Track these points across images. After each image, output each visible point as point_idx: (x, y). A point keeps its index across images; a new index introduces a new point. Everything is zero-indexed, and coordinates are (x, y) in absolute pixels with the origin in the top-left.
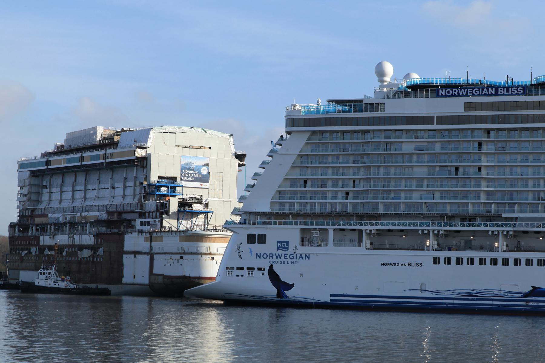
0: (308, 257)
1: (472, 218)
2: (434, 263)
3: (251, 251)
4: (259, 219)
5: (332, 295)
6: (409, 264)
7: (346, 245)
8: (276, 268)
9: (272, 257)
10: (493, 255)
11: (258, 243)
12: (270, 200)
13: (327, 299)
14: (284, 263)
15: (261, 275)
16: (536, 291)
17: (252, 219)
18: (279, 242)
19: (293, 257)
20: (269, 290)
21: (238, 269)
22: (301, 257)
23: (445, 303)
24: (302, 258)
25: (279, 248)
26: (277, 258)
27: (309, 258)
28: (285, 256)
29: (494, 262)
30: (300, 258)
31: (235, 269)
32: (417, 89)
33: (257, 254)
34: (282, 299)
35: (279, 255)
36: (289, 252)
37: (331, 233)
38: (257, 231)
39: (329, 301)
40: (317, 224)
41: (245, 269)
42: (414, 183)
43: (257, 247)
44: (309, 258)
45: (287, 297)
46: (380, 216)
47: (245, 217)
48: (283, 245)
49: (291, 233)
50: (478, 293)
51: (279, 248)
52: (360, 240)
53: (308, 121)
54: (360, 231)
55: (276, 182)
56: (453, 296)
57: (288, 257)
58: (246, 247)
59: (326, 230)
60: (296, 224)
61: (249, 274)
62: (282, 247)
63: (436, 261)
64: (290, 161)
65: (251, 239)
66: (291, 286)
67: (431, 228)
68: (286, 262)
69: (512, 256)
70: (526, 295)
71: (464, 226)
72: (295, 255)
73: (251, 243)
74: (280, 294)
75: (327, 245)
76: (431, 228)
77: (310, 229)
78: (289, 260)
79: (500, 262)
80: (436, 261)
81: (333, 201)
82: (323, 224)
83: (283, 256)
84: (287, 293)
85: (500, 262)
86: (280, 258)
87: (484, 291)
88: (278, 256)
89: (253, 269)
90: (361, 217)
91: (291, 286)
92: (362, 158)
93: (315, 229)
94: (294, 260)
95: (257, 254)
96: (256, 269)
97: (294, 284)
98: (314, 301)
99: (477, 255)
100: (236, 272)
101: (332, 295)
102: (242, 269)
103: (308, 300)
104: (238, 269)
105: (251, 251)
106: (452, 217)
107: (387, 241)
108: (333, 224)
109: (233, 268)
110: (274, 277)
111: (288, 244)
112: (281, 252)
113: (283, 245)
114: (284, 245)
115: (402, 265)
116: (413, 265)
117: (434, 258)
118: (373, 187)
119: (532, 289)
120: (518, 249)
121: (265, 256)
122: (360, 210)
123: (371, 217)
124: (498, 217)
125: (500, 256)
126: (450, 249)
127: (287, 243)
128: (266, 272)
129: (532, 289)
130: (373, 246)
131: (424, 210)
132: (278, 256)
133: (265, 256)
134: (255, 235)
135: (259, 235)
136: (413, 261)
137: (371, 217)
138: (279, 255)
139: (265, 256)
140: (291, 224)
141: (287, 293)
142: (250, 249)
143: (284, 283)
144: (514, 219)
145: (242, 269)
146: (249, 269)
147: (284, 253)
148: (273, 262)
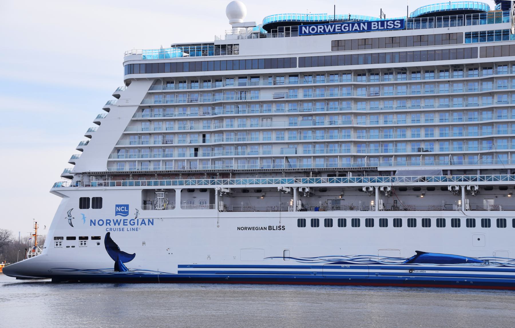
0: (151, 222)
1: (343, 173)
2: (299, 226)
3: (84, 218)
4: (94, 180)
5: (180, 266)
6: (270, 228)
7: (196, 208)
8: (114, 237)
9: (109, 223)
10: (369, 214)
11: (93, 207)
12: (107, 159)
13: (174, 271)
14: (123, 230)
15: (96, 245)
16: (420, 257)
17: (86, 180)
18: (117, 206)
19: (134, 223)
20: (105, 263)
21: (69, 238)
22: (143, 222)
23: (312, 273)
24: (145, 223)
25: (117, 213)
26: (115, 224)
27: (152, 224)
28: (124, 222)
29: (370, 223)
30: (142, 223)
31: (65, 238)
32: (273, 28)
33: (91, 221)
34: (121, 273)
35: (117, 220)
36: (129, 218)
37: (178, 194)
38: (91, 194)
39: (177, 273)
40: (162, 184)
41: (77, 238)
42: (271, 136)
43: (91, 213)
44: (152, 224)
45: (126, 269)
46: (235, 174)
47: (76, 179)
48: (123, 210)
49: (132, 195)
50: (352, 260)
51: (117, 213)
52: (212, 201)
53: (150, 68)
54: (212, 191)
55: (112, 136)
56: (322, 264)
57: (128, 223)
58: (78, 212)
59: (173, 191)
60: (137, 184)
61: (82, 244)
62: (121, 212)
63: (302, 223)
64: (130, 113)
65: (84, 203)
66: (130, 257)
67: (295, 185)
68: (125, 229)
69: (391, 215)
70: (410, 261)
71: (333, 182)
72: (136, 221)
73: (84, 208)
74: (118, 267)
75: (174, 208)
76: (295, 185)
77: (153, 191)
78: (129, 226)
79: (377, 223)
80: (302, 223)
81: (180, 158)
82: (169, 184)
83: (122, 222)
84: (127, 265)
85: (377, 223)
86: (119, 224)
87: (359, 257)
88: (117, 222)
89: (86, 238)
90: (212, 174)
91: (130, 257)
92: (213, 109)
93: (159, 190)
94: (136, 226)
95: (91, 221)
96: (90, 238)
97: (135, 254)
98: (159, 273)
99: (349, 215)
100: (65, 242)
101: (180, 266)
102: (74, 238)
103: (152, 273)
104: (69, 238)
105: (84, 218)
106: (318, 173)
107: (242, 203)
108: (181, 184)
109: (62, 238)
110: (111, 247)
111: (128, 209)
112: (119, 217)
113: (123, 210)
114: (123, 209)
115: (262, 228)
116: (275, 228)
117: (299, 220)
118: (226, 141)
119: (416, 254)
120: (395, 208)
121: (101, 223)
122: (209, 167)
123: (224, 174)
124: (372, 171)
125: (377, 215)
126: (317, 209)
127: (127, 206)
128: (102, 241)
129: (416, 254)
130: (227, 209)
131: (283, 165)
132: (117, 222)
133: (101, 223)
134: (89, 198)
135: (93, 198)
136: (275, 224)
137: (224, 174)
138: (117, 220)
139: (101, 223)
140: (131, 184)
141: (127, 265)
142: (84, 215)
144: (392, 173)
145: (74, 238)
146: (81, 238)
147: (123, 218)
148: (111, 229)
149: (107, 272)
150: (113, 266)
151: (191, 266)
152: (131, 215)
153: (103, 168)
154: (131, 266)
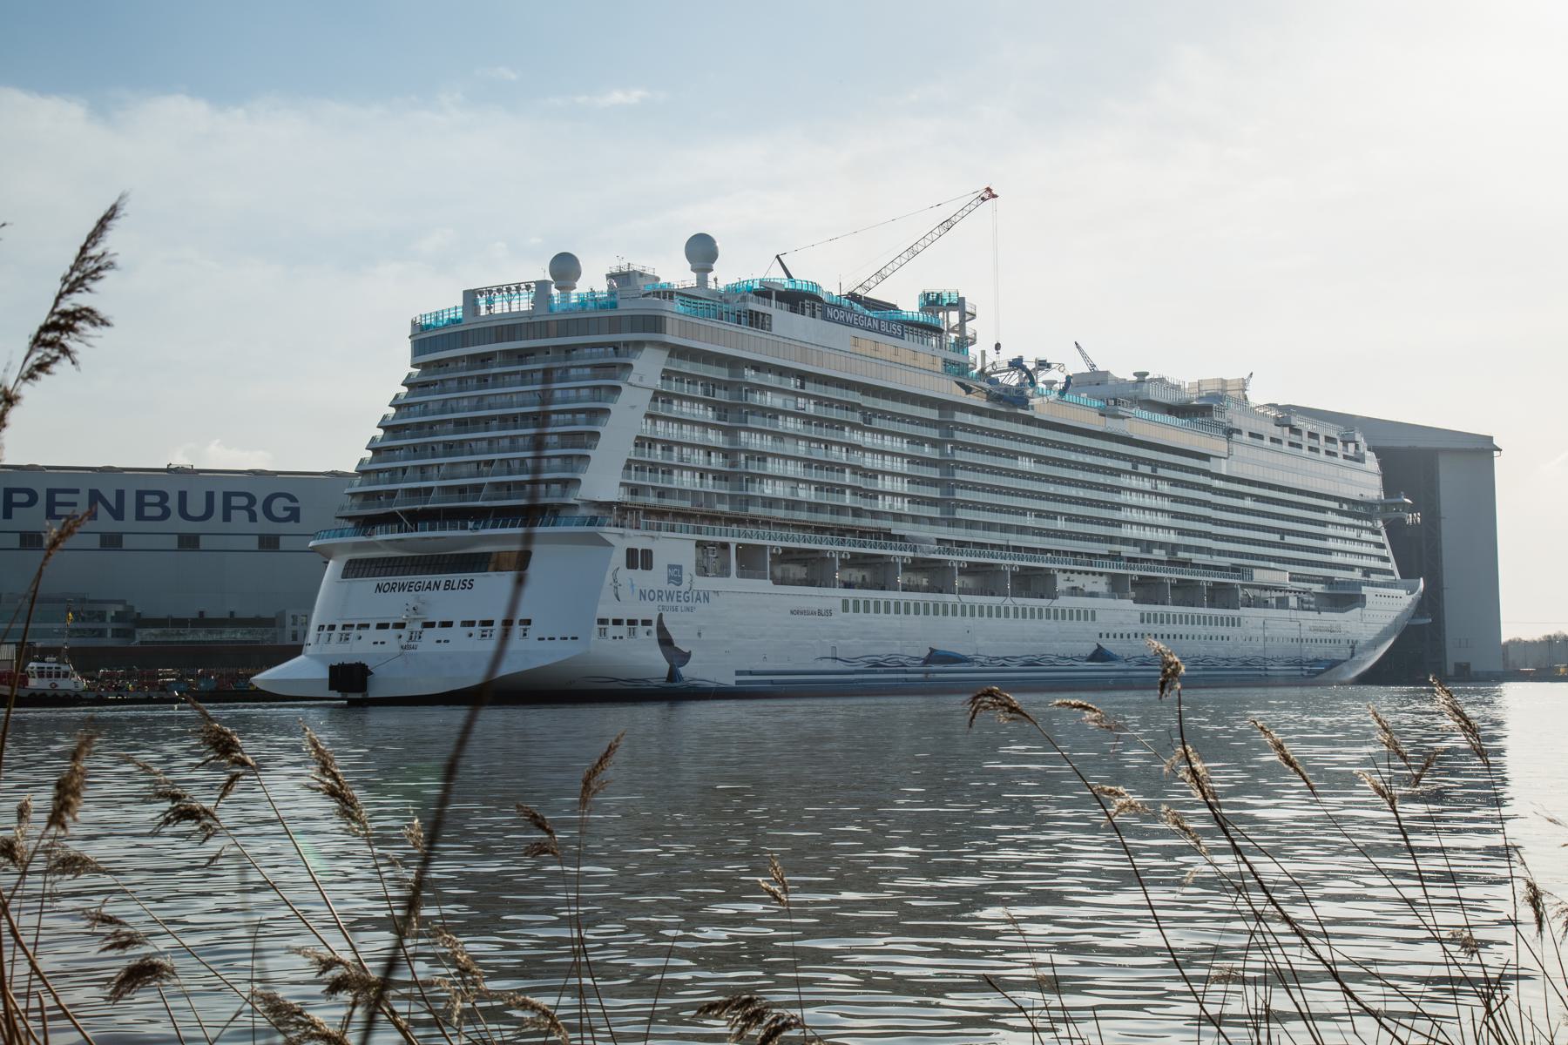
13: (730, 681)
16: (935, 657)
18: (670, 567)
22: (698, 599)
39: (733, 684)
45: (681, 678)
58: (626, 575)
74: (673, 675)
87: (890, 657)
88: (670, 596)
91: (687, 656)
94: (690, 604)
100: (612, 630)
101: (738, 673)
110: (665, 641)
112: (672, 587)
113: (675, 574)
127: (680, 567)
128: (654, 628)
132: (670, 596)
141: (683, 671)
143: (677, 649)
151: (751, 673)
152: (685, 586)
154: (687, 672)
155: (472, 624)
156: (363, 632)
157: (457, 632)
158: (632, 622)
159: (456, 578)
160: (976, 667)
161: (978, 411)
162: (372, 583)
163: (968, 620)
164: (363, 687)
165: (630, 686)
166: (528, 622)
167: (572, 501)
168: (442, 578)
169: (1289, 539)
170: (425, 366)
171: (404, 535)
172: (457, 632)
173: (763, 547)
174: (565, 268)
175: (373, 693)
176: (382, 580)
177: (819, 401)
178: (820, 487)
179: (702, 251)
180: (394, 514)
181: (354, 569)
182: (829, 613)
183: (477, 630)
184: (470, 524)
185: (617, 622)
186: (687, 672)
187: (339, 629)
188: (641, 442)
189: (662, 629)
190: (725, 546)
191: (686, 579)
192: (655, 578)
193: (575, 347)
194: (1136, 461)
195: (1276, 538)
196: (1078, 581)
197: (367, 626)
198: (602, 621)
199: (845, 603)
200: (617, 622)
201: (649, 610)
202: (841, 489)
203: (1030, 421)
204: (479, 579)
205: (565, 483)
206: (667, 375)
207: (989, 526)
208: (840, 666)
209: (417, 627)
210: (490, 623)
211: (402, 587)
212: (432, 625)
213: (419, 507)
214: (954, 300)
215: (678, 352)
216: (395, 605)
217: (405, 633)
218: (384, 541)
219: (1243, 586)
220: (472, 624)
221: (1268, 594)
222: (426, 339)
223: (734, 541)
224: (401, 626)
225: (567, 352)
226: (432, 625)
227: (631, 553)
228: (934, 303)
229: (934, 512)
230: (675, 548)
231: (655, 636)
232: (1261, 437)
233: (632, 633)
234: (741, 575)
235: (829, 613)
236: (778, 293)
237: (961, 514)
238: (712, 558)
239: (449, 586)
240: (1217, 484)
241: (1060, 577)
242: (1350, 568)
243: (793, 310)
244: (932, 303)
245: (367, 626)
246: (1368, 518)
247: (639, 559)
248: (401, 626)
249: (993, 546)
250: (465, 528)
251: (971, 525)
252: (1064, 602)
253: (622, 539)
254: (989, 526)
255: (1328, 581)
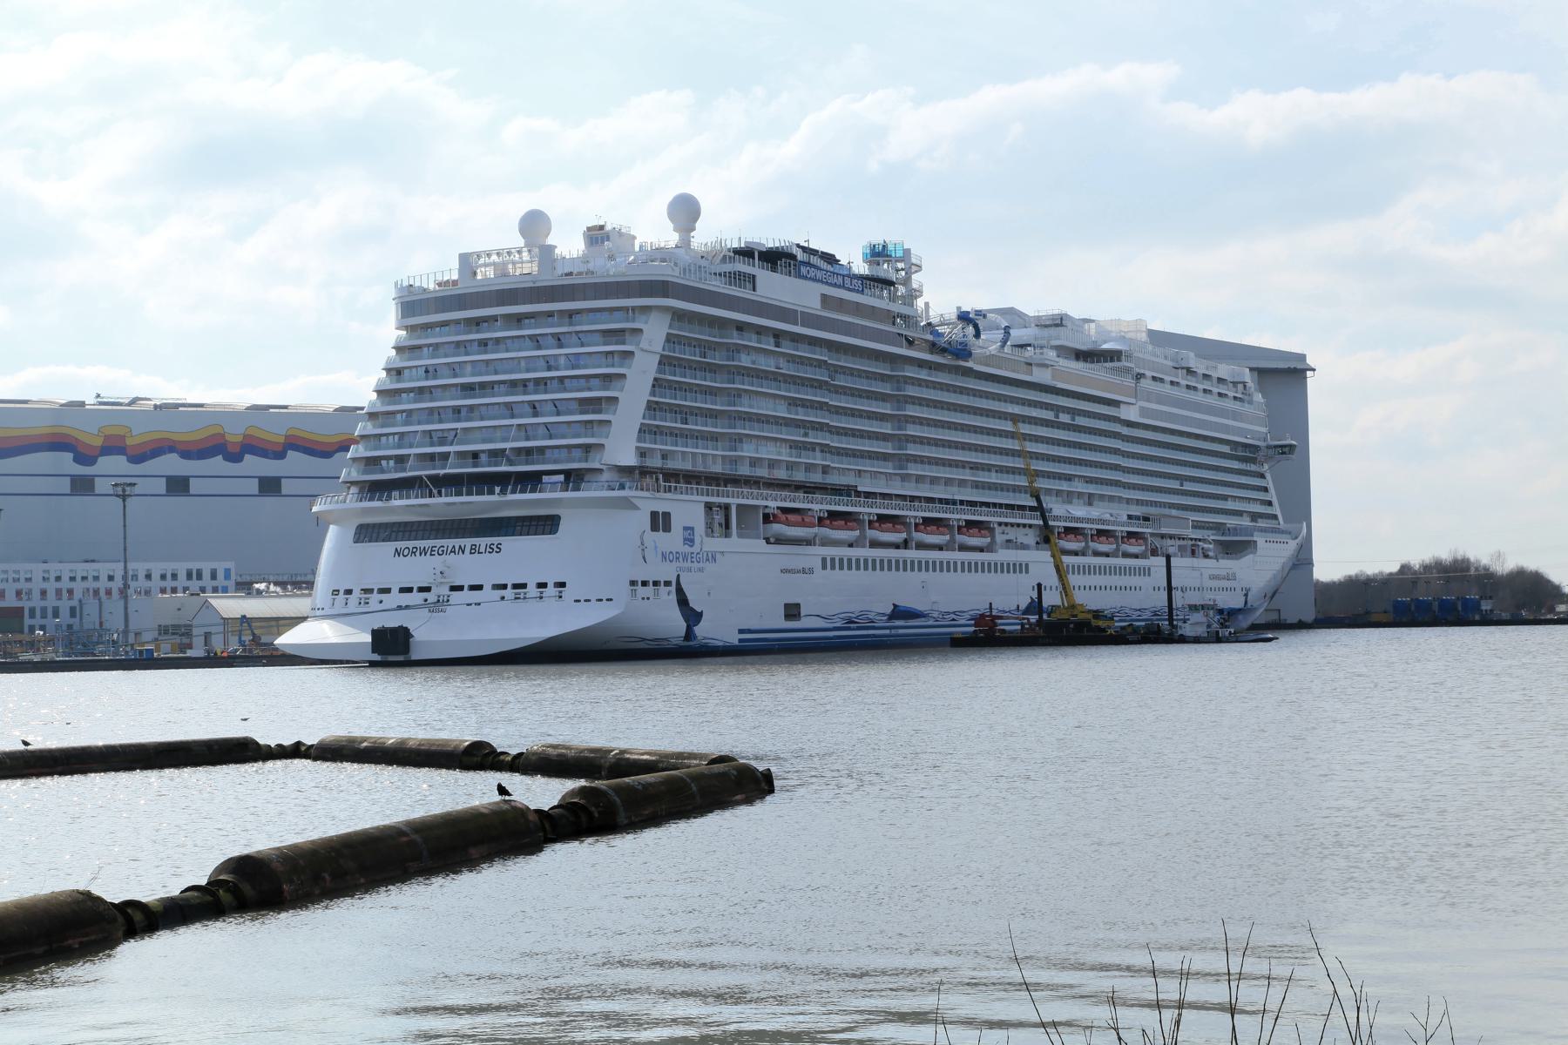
13: (733, 639)
16: (898, 613)
18: (686, 529)
58: (651, 537)
74: (689, 634)
87: (863, 613)
97: (701, 614)
101: (741, 631)
110: (683, 601)
112: (687, 549)
127: (692, 529)
128: (673, 588)
132: (685, 558)
149: (675, 641)
150: (683, 632)
152: (696, 549)
153: (630, 460)
155: (504, 587)
156: (383, 597)
157: (488, 594)
158: (656, 583)
159: (483, 542)
160: (931, 623)
161: (921, 364)
162: (391, 546)
163: (923, 575)
164: (406, 648)
165: (653, 645)
166: (563, 585)
167: (596, 465)
168: (467, 542)
169: (1188, 486)
170: (411, 329)
171: (427, 501)
172: (488, 594)
173: (756, 507)
174: (534, 224)
175: (415, 656)
176: (401, 545)
177: (792, 359)
178: (794, 445)
179: (686, 211)
180: (420, 478)
181: (367, 533)
182: (811, 571)
183: (509, 593)
184: (497, 489)
185: (644, 584)
186: (701, 631)
187: (357, 593)
188: (652, 407)
189: (680, 591)
190: (727, 508)
191: (697, 540)
192: (672, 541)
193: (578, 312)
194: (1058, 409)
195: (1175, 485)
196: (1012, 534)
197: (388, 591)
198: (633, 583)
199: (824, 560)
200: (644, 584)
201: (667, 572)
202: (812, 447)
203: (968, 372)
204: (508, 543)
205: (587, 448)
206: (670, 339)
207: (934, 481)
208: (821, 623)
209: (445, 591)
210: (524, 586)
211: (424, 552)
212: (460, 588)
213: (442, 472)
214: (900, 254)
215: (679, 316)
216: (419, 567)
217: (431, 597)
218: (401, 506)
219: (1152, 535)
220: (504, 587)
221: (1170, 542)
222: (413, 304)
223: (734, 501)
224: (428, 589)
225: (571, 316)
226: (460, 588)
227: (654, 515)
228: (878, 254)
229: (889, 468)
230: (688, 509)
231: (673, 597)
232: (1154, 378)
233: (657, 594)
234: (740, 536)
235: (811, 571)
236: (761, 253)
237: (914, 470)
238: (721, 520)
239: (474, 550)
240: (1125, 431)
241: (998, 530)
242: (1239, 513)
243: (774, 270)
244: (878, 254)
245: (388, 591)
246: (1253, 461)
247: (660, 522)
248: (428, 589)
249: (941, 501)
250: (491, 492)
251: (919, 479)
252: (1003, 555)
253: (649, 501)
254: (934, 481)
255: (1218, 527)
